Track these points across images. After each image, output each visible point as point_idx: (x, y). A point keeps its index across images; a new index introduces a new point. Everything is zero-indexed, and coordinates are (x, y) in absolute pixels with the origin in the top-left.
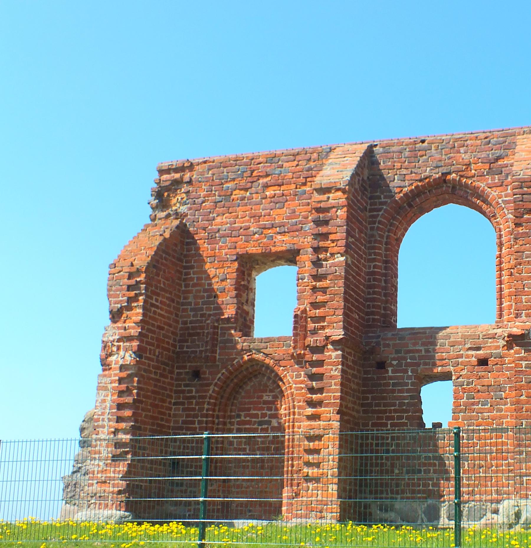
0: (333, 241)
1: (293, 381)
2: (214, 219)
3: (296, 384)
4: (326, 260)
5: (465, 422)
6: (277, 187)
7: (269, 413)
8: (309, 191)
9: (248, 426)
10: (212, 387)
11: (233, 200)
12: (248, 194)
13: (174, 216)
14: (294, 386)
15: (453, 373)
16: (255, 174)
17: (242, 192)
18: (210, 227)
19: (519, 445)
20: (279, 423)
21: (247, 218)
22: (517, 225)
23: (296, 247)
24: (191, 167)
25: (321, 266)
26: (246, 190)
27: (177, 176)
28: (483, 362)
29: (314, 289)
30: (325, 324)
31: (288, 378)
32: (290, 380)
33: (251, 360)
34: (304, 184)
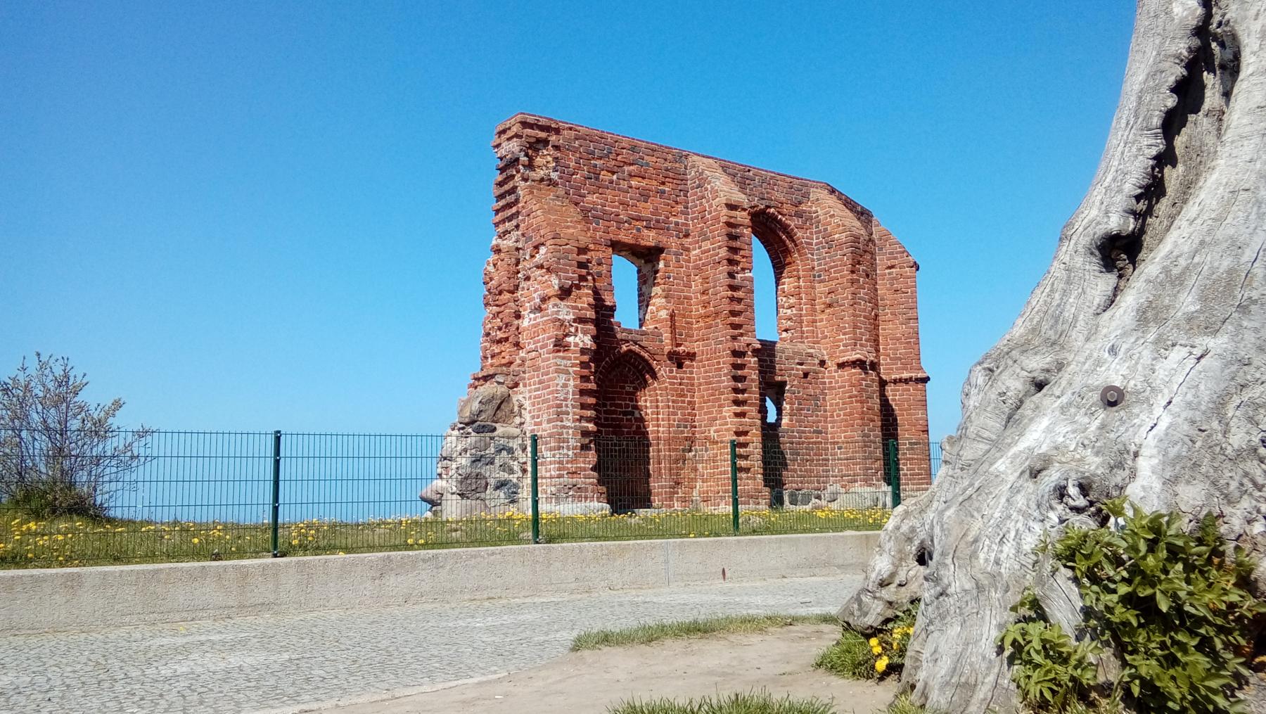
0: (743, 257)
2: (585, 197)
4: (737, 273)
6: (640, 179)
7: (631, 403)
12: (615, 177)
13: (548, 182)
16: (619, 158)
17: (609, 174)
19: (865, 446)
20: (641, 414)
21: (617, 203)
22: (853, 272)
23: (661, 245)
24: (557, 131)
25: (734, 277)
26: (613, 173)
27: (542, 135)
28: (806, 375)
29: (732, 299)
30: (741, 331)
31: (662, 372)
33: (630, 351)
34: (663, 183)
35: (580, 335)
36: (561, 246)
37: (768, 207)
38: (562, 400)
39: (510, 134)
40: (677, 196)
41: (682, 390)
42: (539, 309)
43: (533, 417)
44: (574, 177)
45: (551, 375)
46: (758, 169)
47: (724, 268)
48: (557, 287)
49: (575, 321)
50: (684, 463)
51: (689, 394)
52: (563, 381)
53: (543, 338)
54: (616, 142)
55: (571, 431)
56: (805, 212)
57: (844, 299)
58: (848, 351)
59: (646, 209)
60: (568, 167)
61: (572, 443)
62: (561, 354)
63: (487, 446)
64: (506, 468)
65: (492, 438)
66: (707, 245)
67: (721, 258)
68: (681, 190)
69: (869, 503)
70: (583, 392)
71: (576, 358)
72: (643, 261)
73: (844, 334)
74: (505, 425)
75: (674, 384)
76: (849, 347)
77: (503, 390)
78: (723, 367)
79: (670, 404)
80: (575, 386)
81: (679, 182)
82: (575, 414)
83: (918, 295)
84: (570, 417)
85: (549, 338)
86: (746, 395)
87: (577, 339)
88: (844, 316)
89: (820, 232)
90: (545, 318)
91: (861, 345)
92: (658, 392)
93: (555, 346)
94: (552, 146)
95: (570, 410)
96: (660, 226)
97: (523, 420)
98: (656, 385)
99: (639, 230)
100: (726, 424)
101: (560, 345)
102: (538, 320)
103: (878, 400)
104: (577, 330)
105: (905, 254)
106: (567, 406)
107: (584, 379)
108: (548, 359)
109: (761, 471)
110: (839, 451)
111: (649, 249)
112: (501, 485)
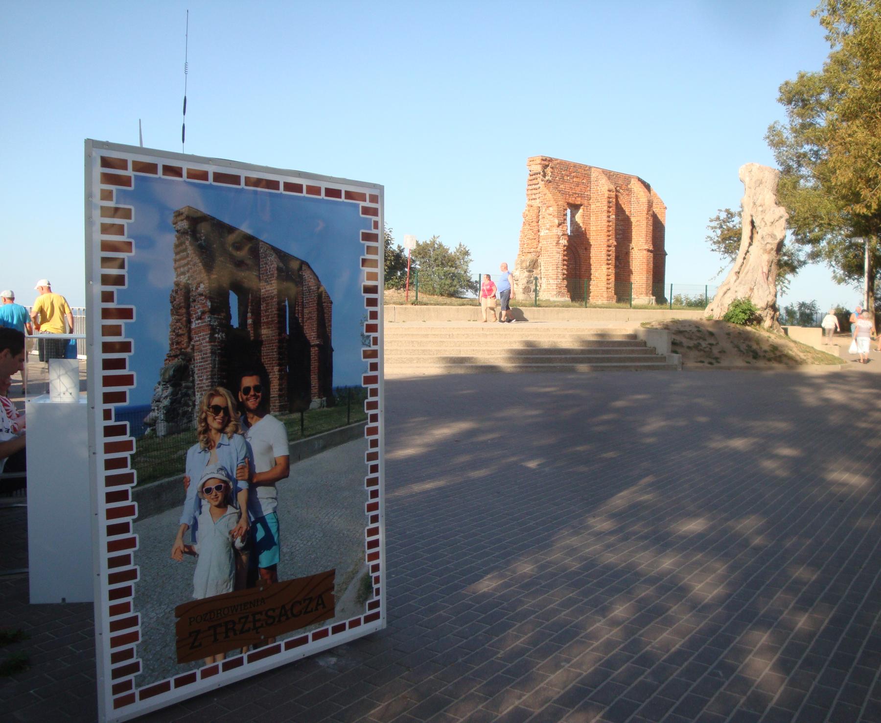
47: (605, 214)
49: (562, 235)
59: (578, 190)
63: (531, 277)
69: (647, 302)
101: (558, 243)
107: (564, 255)
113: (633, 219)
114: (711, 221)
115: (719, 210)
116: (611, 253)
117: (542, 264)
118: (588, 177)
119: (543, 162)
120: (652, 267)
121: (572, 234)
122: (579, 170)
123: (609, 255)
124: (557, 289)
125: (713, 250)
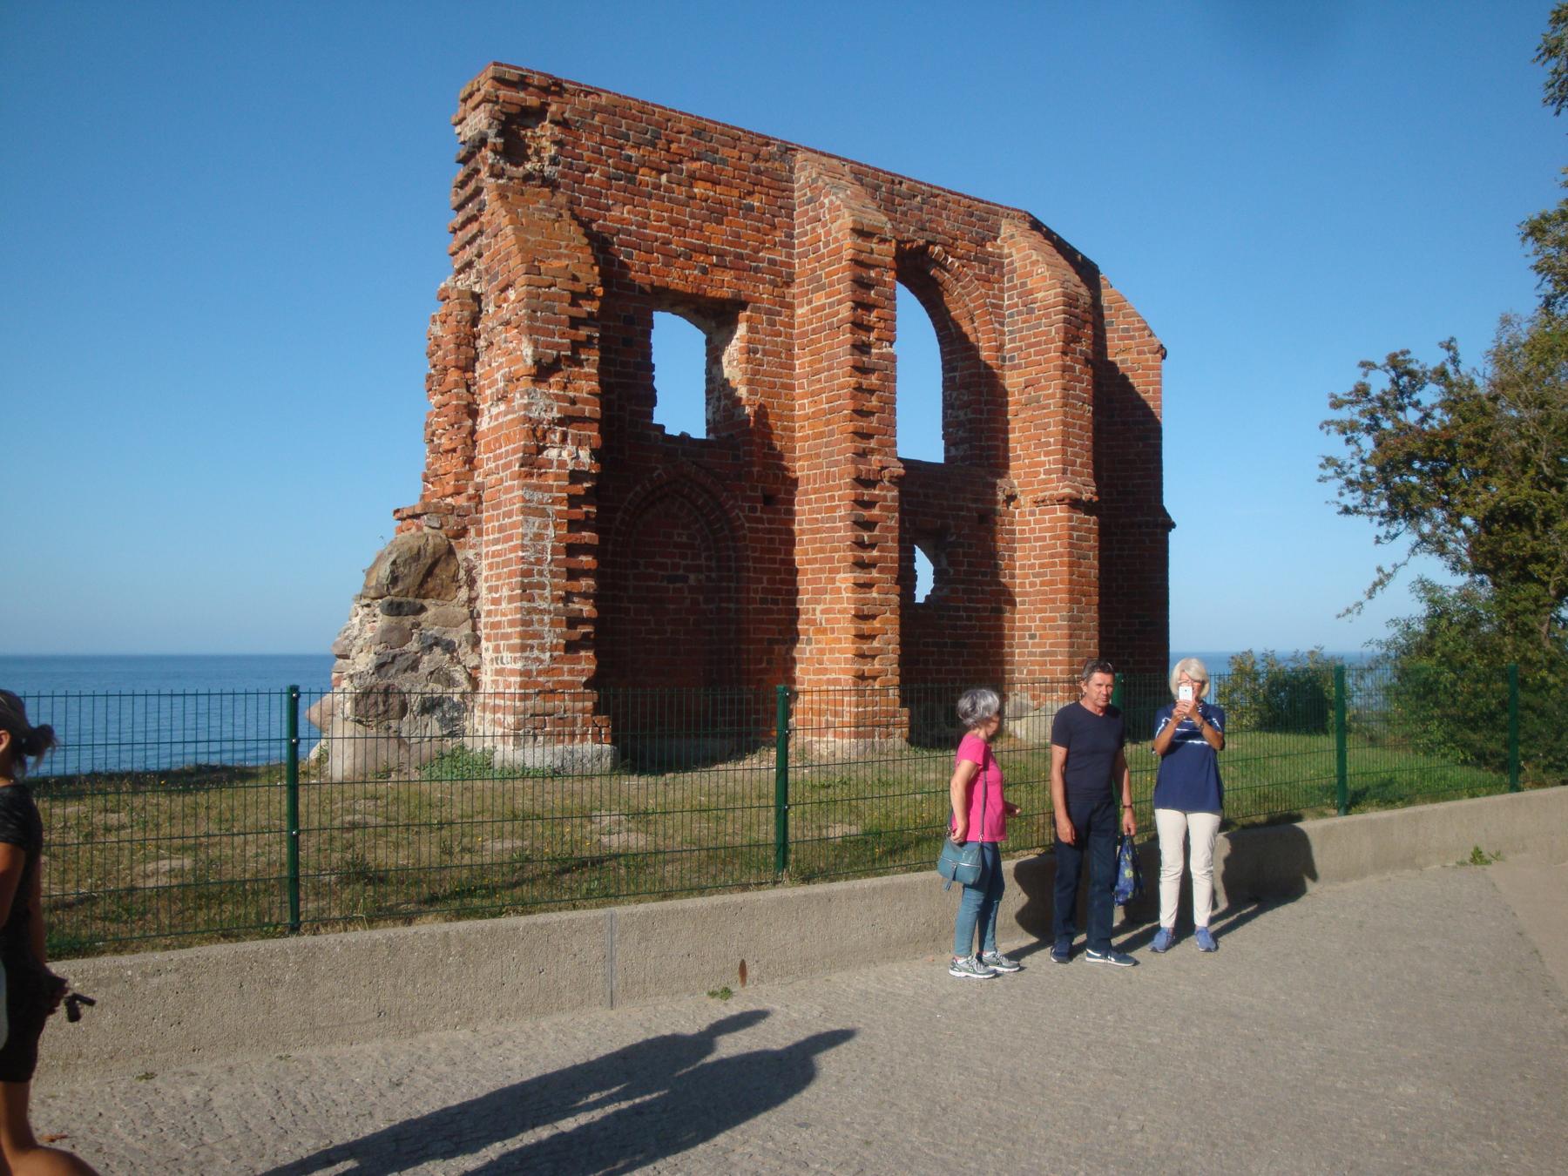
1: (745, 517)
3: (749, 522)
5: (965, 597)
6: (709, 184)
8: (758, 208)
9: (652, 584)
10: (619, 515)
11: (640, 184)
12: (664, 178)
14: (747, 525)
15: (953, 530)
18: (601, 222)
21: (665, 224)
26: (661, 172)
32: (741, 514)
34: (750, 193)
35: (570, 447)
36: (539, 287)
37: (929, 243)
38: (531, 563)
39: (477, 97)
40: (774, 216)
41: (772, 541)
42: (503, 397)
43: (490, 589)
44: (589, 175)
45: (515, 518)
46: (916, 182)
47: (846, 337)
48: (529, 361)
49: (561, 422)
50: (769, 662)
51: (783, 547)
52: (535, 530)
53: (507, 451)
54: (669, 120)
55: (546, 618)
56: (991, 255)
57: (1048, 397)
58: (1051, 481)
59: (718, 234)
60: (580, 157)
61: (548, 641)
62: (534, 481)
63: (407, 638)
64: (437, 674)
65: (417, 625)
66: (820, 299)
67: (841, 320)
68: (780, 208)
70: (572, 550)
71: (561, 489)
72: (714, 324)
73: (1047, 454)
74: (439, 602)
75: (757, 531)
76: (1054, 476)
77: (438, 540)
78: (839, 506)
79: (750, 564)
80: (558, 538)
81: (778, 193)
82: (554, 587)
83: (1164, 396)
84: (547, 592)
85: (515, 451)
86: (875, 553)
87: (565, 454)
88: (1048, 424)
89: (1014, 288)
90: (510, 417)
91: (1073, 473)
92: (730, 544)
93: (522, 466)
94: (552, 122)
95: (546, 580)
96: (740, 265)
97: (474, 594)
98: (727, 532)
99: (704, 271)
100: (840, 601)
102: (500, 420)
103: (1096, 563)
104: (564, 439)
105: (1146, 333)
106: (541, 573)
107: (574, 525)
108: (510, 489)
109: (897, 680)
110: (1030, 642)
111: (722, 302)
112: (430, 706)
113: (1012, 381)
114: (1337, 404)
115: (1363, 364)
116: (876, 511)
117: (483, 570)
118: (780, 187)
119: (504, 93)
120: (1094, 573)
121: (712, 437)
122: (724, 152)
123: (868, 525)
124: (524, 697)
125: (1346, 510)
